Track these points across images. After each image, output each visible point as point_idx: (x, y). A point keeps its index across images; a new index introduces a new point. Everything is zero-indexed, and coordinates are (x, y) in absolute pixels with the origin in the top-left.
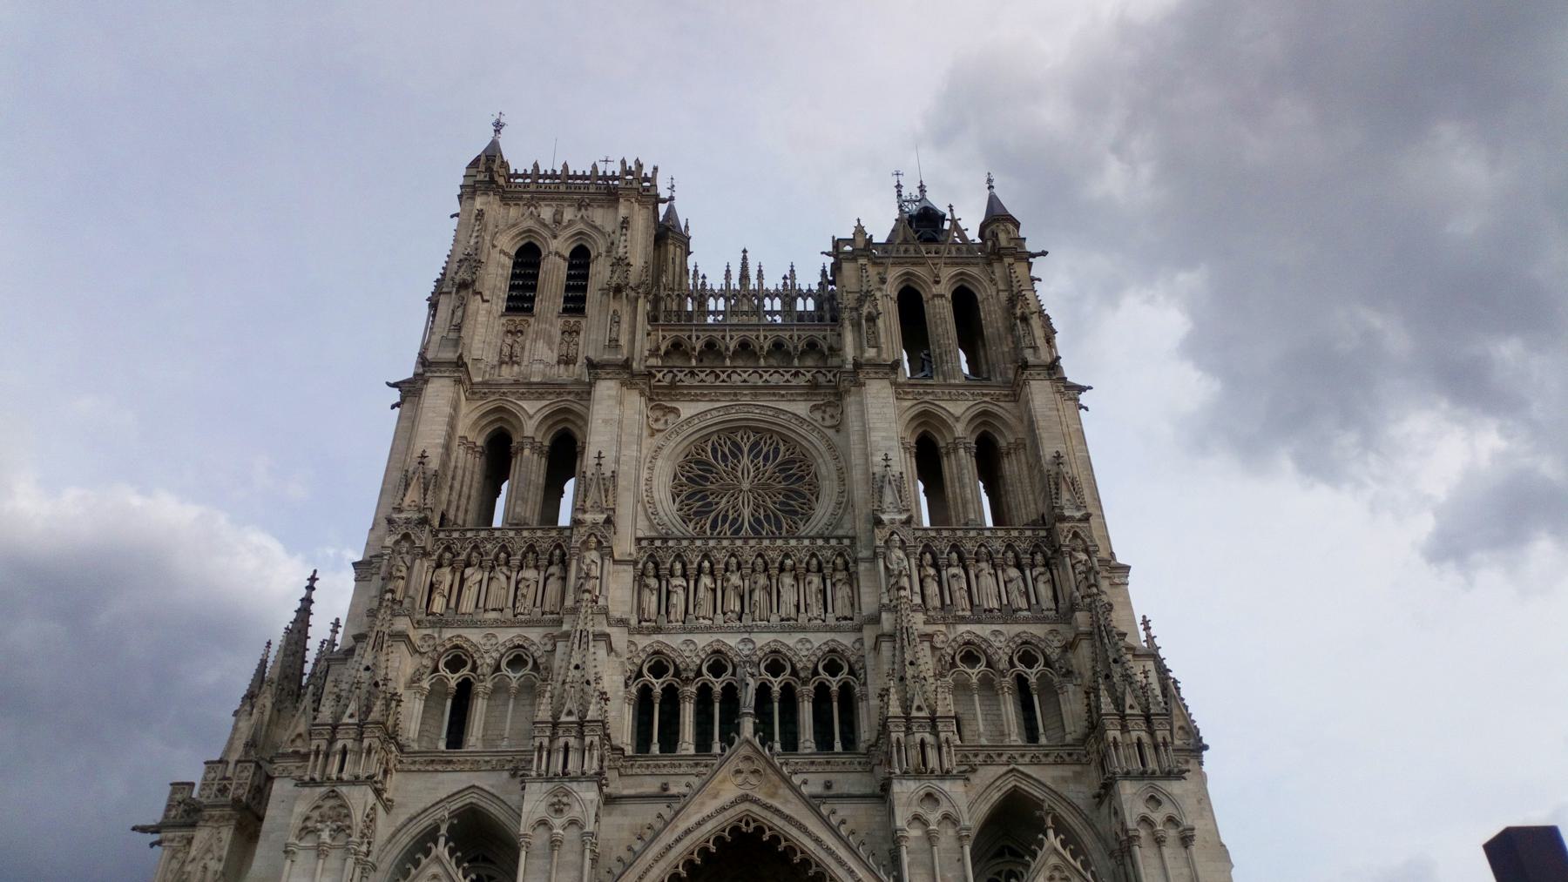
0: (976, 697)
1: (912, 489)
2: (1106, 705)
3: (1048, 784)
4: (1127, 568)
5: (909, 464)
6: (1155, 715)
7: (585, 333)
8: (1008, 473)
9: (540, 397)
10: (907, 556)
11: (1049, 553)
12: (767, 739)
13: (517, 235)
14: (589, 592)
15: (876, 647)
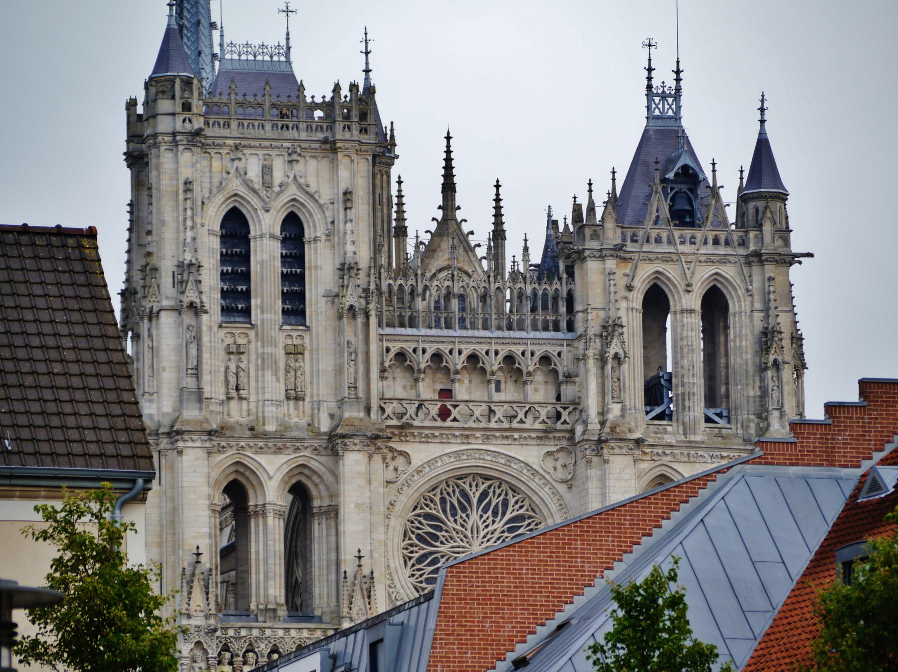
7: (311, 353)
9: (279, 450)
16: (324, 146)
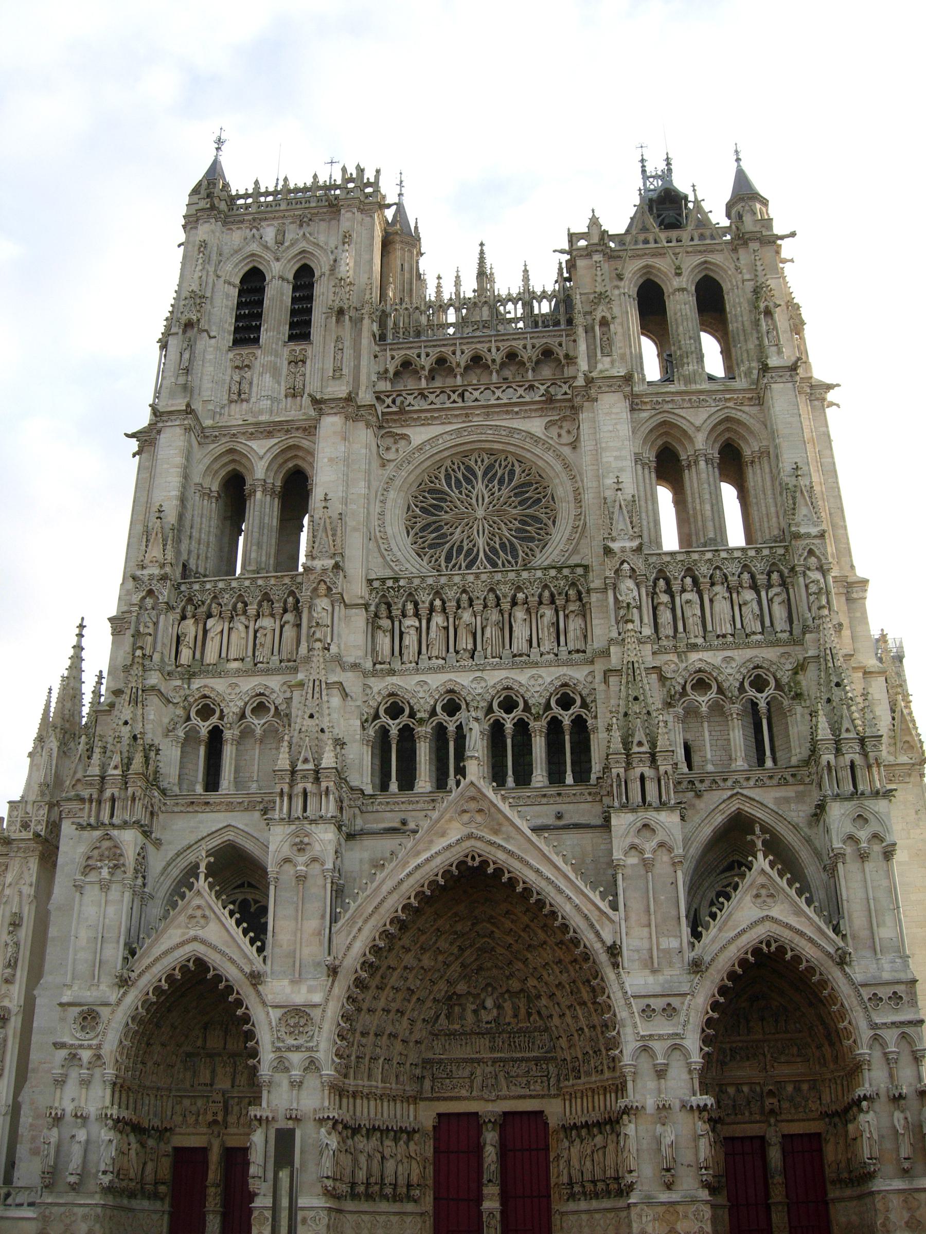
0: (706, 725)
1: (650, 507)
2: (824, 731)
3: (771, 806)
4: (864, 582)
5: (647, 481)
6: (868, 737)
8: (752, 484)
9: (270, 434)
10: (638, 585)
11: (786, 571)
12: (498, 777)
13: (240, 262)
14: (320, 640)
15: (606, 681)
16: (330, 209)
